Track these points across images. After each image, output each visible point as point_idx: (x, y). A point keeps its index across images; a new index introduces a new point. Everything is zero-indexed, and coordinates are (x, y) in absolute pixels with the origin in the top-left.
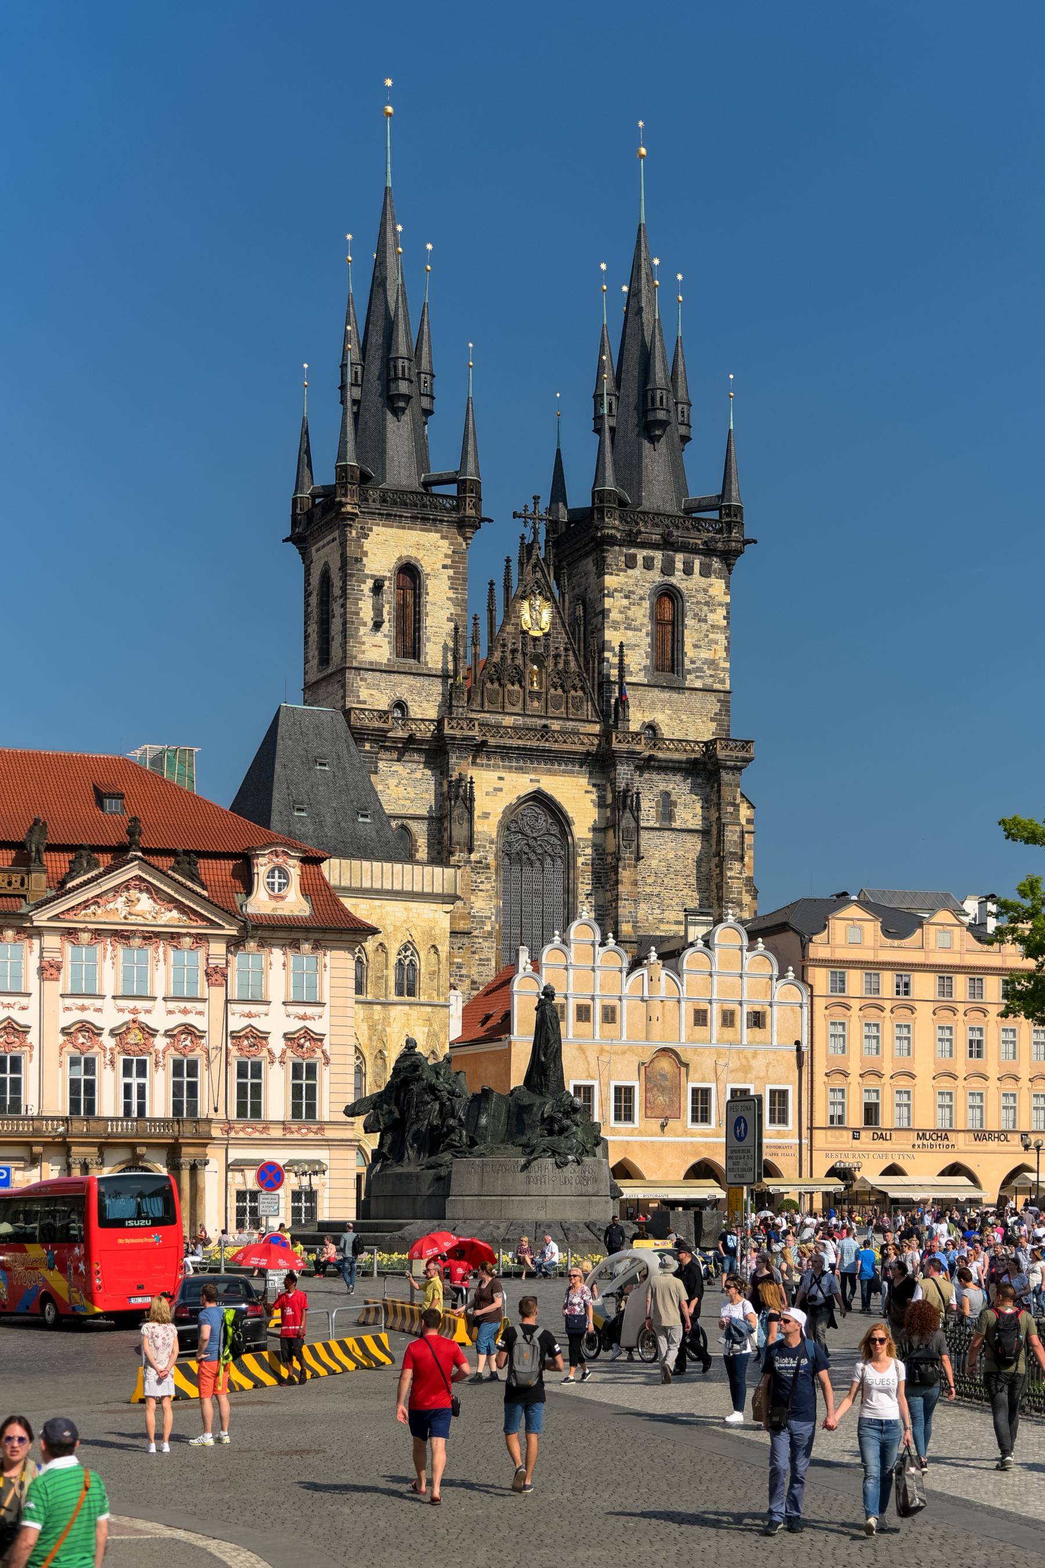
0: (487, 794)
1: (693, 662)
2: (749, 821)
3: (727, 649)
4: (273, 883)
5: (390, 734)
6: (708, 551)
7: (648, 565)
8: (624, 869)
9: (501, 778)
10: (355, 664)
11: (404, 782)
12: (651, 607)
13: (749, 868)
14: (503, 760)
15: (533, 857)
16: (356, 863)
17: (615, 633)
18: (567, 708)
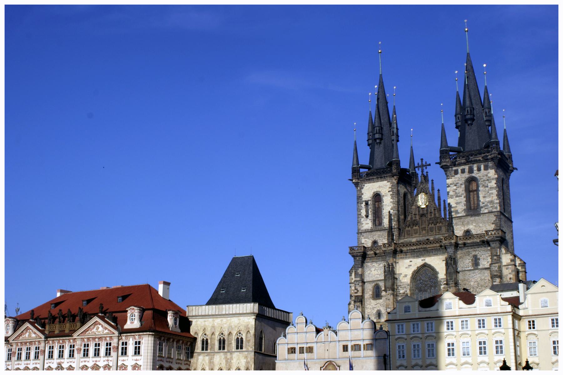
0: (406, 268)
1: (483, 203)
2: (512, 261)
3: (497, 195)
4: (133, 319)
5: (368, 253)
6: (486, 160)
7: (463, 171)
8: (450, 288)
9: (411, 261)
10: (360, 231)
11: (377, 269)
12: (466, 187)
13: (513, 279)
14: (411, 254)
15: (426, 288)
16: (221, 306)
17: (451, 200)
18: (436, 231)
